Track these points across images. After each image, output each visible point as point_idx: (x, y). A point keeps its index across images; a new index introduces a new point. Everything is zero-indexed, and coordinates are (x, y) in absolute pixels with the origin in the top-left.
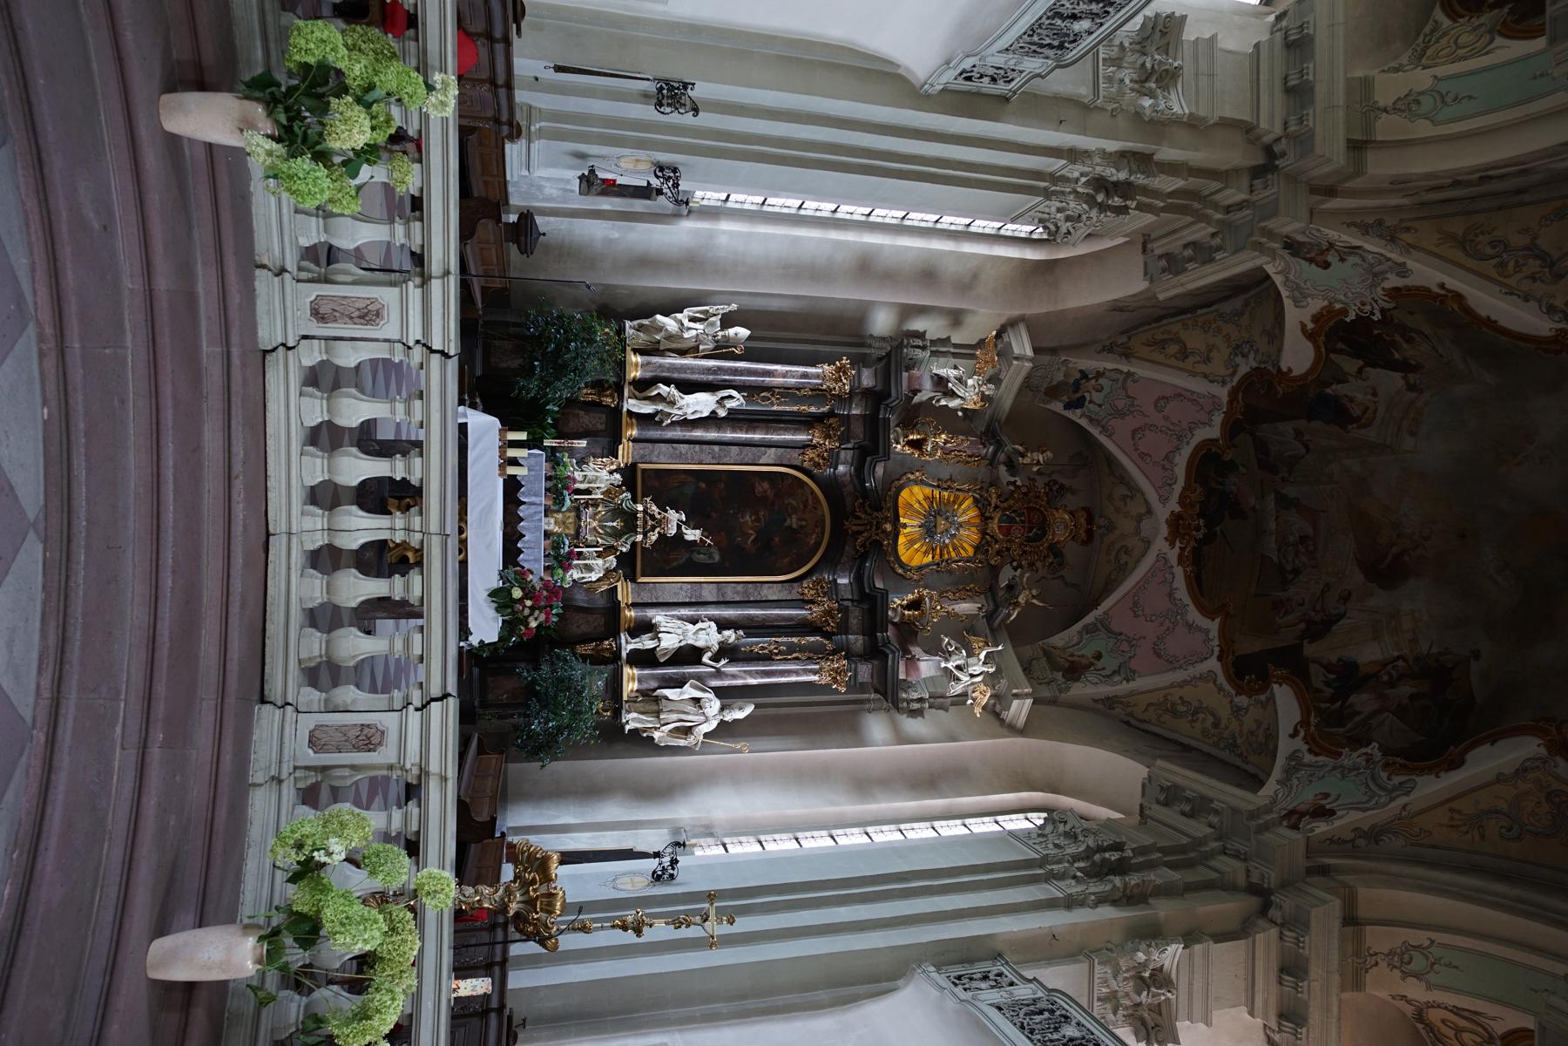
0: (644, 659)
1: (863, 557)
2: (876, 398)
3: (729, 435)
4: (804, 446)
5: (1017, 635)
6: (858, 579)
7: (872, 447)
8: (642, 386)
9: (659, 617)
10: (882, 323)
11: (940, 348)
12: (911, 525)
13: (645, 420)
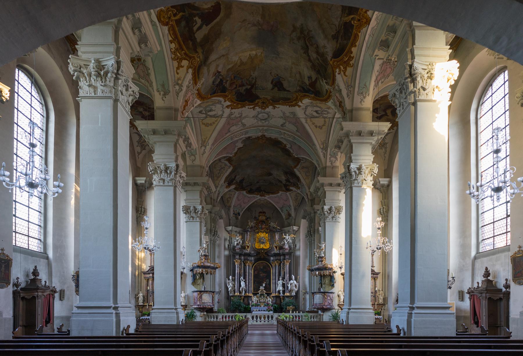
0: (284, 292)
1: (268, 255)
2: (240, 255)
3: (247, 279)
4: (249, 266)
5: (283, 226)
6: (272, 256)
7: (249, 255)
8: (240, 293)
9: (277, 290)
10: (227, 253)
11: (230, 242)
12: (262, 246)
13: (245, 292)
